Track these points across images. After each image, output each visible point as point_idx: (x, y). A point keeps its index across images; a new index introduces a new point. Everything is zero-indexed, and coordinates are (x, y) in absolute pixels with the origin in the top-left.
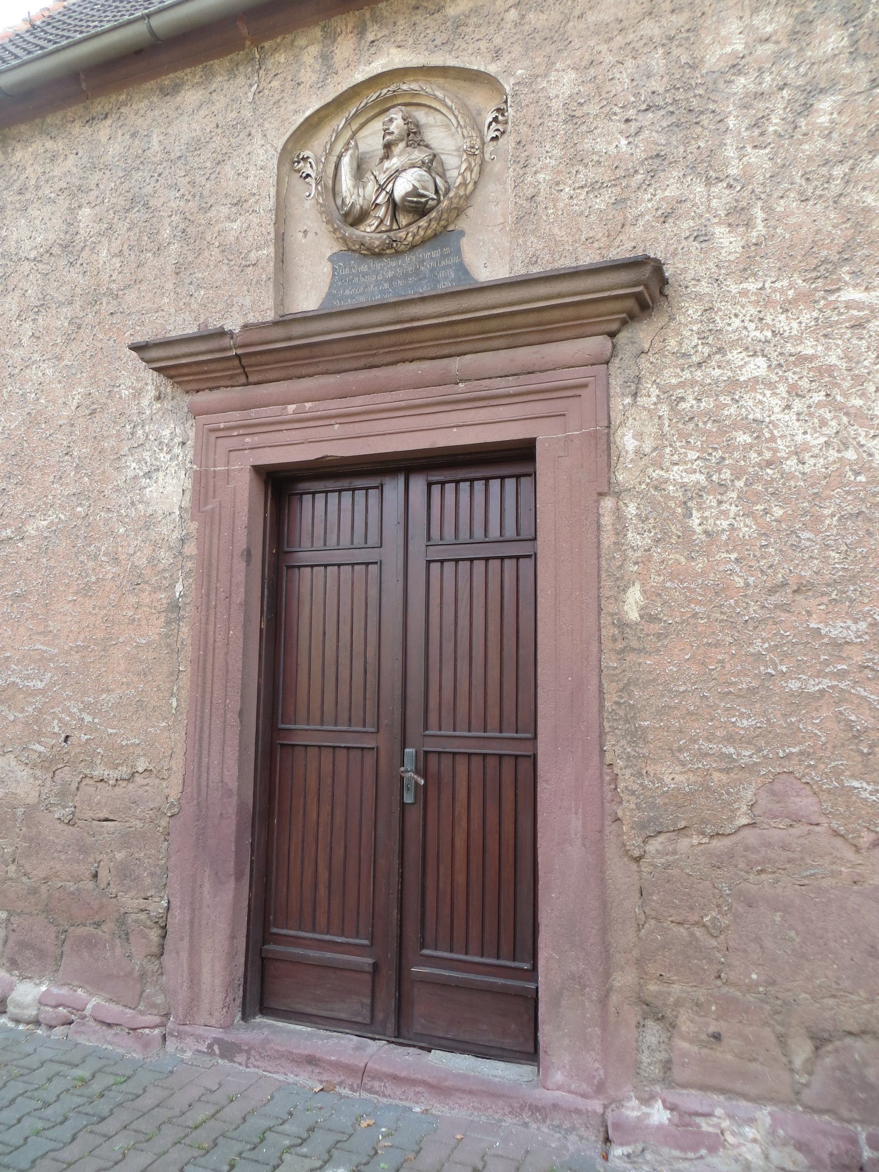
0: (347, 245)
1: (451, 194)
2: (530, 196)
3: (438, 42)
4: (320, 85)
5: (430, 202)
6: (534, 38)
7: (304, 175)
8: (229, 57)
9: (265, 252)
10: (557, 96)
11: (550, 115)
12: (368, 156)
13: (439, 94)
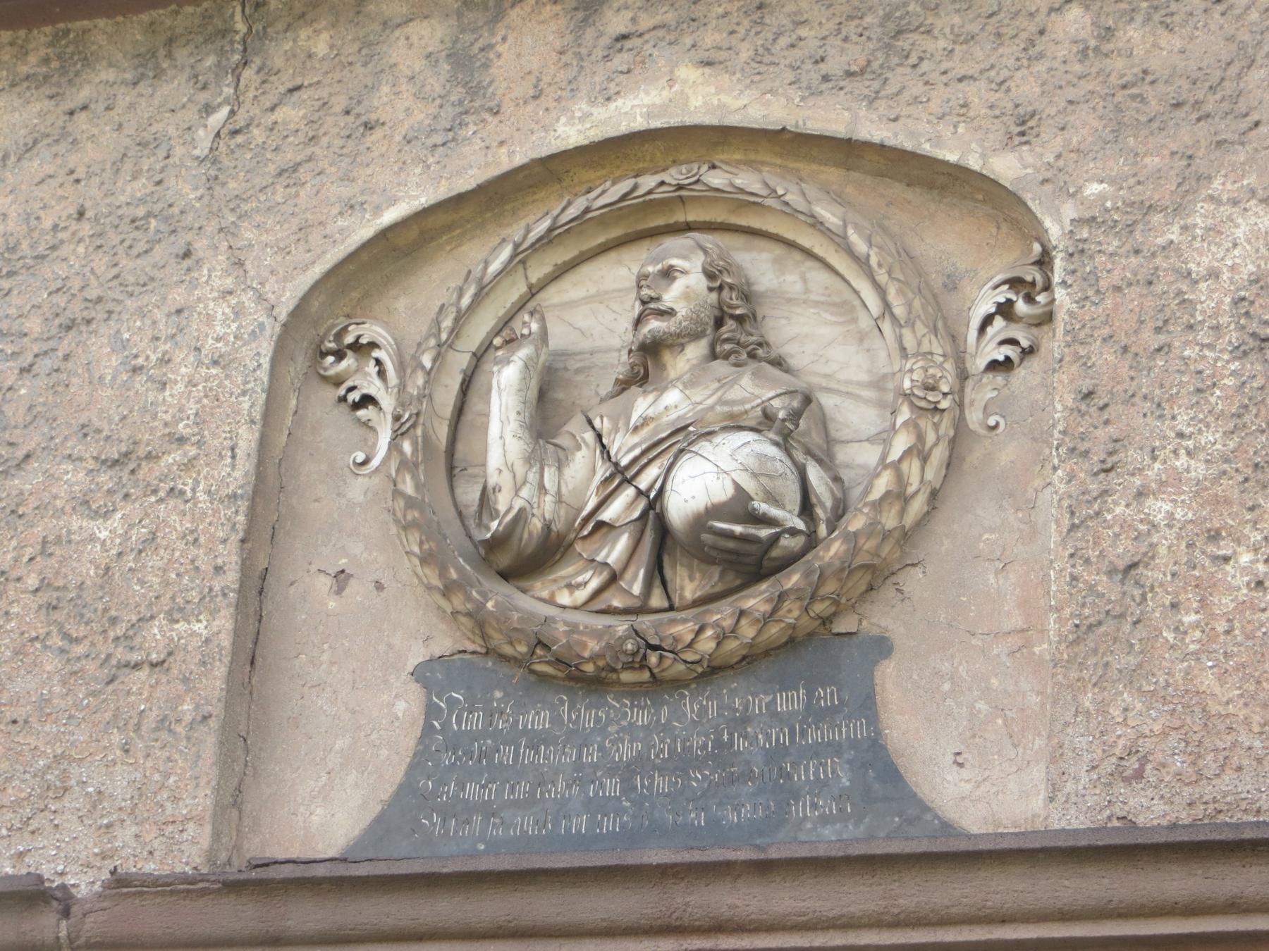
0: (485, 637)
1: (856, 523)
2: (1121, 564)
3: (834, 65)
4: (438, 139)
5: (787, 542)
6: (1142, 99)
7: (355, 396)
8: (145, 17)
9: (199, 627)
10: (1214, 274)
11: (1190, 327)
12: (573, 364)
13: (829, 215)
